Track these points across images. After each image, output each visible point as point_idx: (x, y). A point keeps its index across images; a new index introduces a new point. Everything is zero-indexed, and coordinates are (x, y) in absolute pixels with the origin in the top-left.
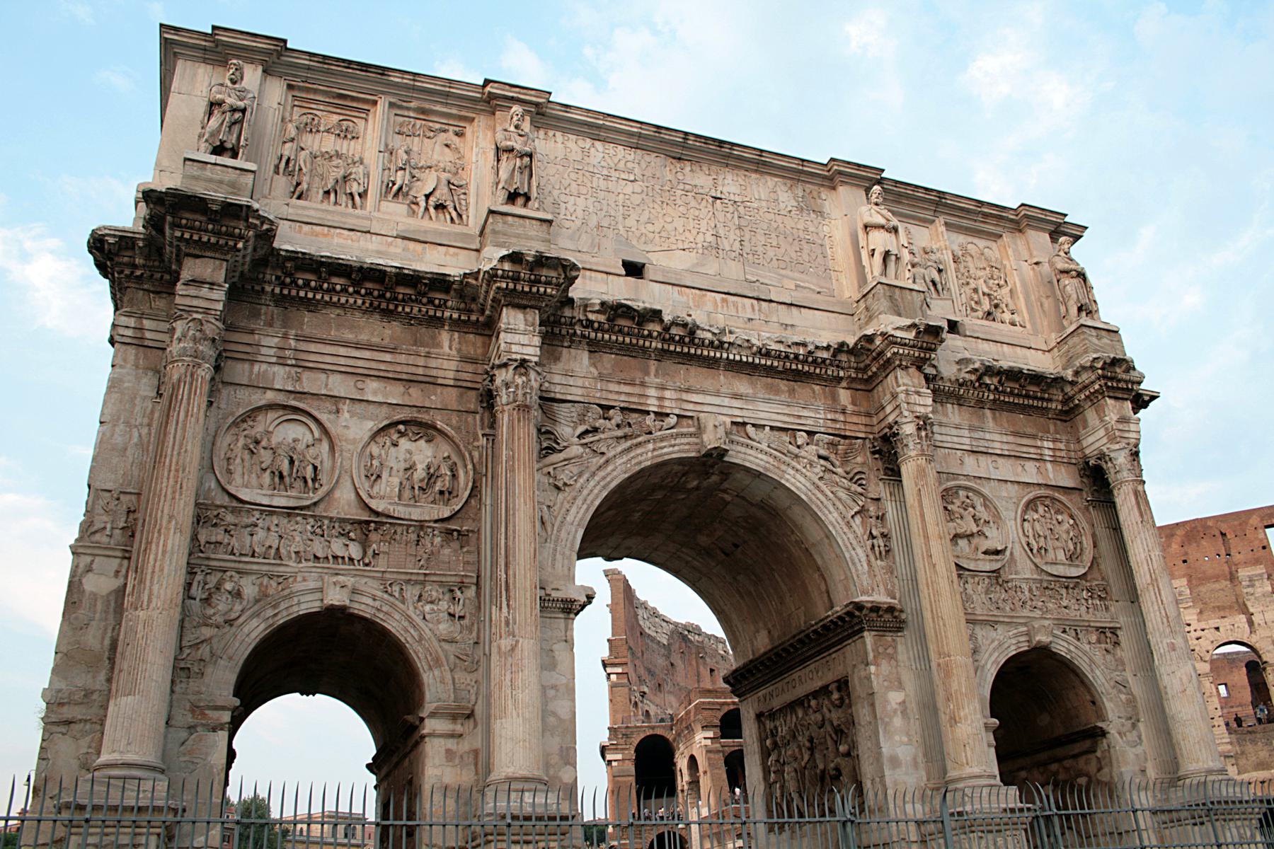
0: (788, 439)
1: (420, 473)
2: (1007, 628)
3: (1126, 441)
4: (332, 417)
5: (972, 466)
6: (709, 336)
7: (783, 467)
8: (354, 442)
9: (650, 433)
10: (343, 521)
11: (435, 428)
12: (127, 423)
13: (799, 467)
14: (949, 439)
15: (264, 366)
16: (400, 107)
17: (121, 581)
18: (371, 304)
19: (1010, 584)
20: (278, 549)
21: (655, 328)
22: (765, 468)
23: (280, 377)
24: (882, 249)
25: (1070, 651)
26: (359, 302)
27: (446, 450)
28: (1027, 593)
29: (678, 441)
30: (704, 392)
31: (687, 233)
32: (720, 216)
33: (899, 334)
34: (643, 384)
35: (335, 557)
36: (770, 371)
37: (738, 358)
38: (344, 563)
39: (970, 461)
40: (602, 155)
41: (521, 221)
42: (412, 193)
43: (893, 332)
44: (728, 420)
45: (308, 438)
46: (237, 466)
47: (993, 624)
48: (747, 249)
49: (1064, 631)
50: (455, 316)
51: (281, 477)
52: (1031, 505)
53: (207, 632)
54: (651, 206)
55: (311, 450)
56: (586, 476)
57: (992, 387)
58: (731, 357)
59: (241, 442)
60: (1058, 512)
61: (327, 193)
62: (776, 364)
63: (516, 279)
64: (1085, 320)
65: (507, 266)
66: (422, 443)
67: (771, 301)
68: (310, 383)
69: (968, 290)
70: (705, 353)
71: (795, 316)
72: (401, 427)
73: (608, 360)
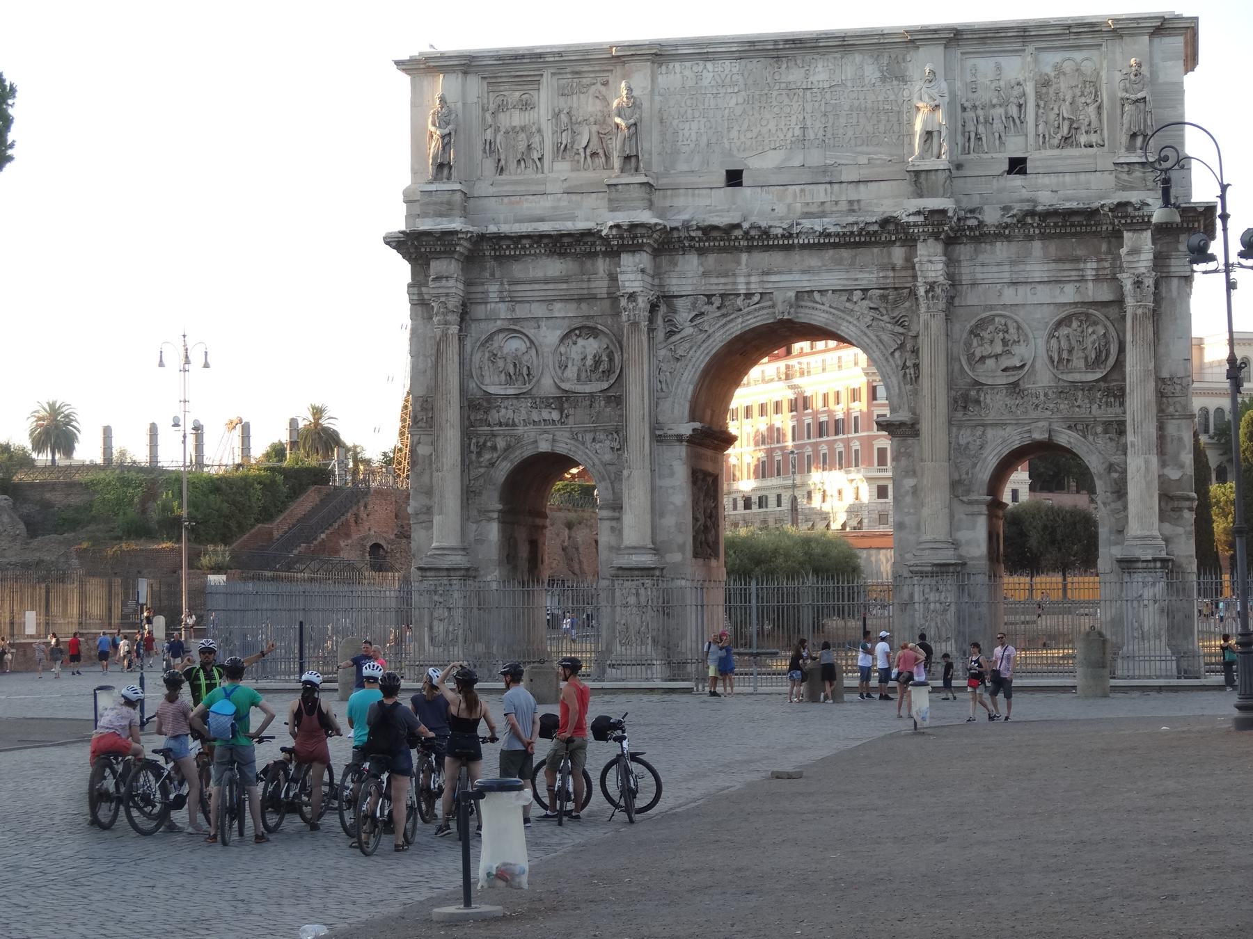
1: (589, 362)
2: (1015, 427)
3: (1133, 271)
6: (780, 231)
7: (839, 321)
9: (741, 310)
10: (547, 398)
11: (596, 328)
12: (424, 355)
13: (851, 320)
14: (990, 276)
15: (493, 305)
19: (1026, 393)
21: (738, 233)
22: (826, 324)
23: (503, 310)
25: (1070, 442)
27: (605, 342)
28: (1042, 397)
29: (761, 313)
31: (779, 132)
32: (809, 107)
33: (912, 219)
34: (734, 275)
36: (835, 246)
37: (806, 241)
40: (712, 74)
41: (627, 187)
42: (576, 147)
43: (905, 219)
44: (792, 294)
45: (524, 348)
46: (486, 373)
47: (1001, 425)
48: (829, 135)
49: (1069, 428)
50: (603, 249)
53: (482, 470)
55: (526, 358)
57: (1035, 225)
58: (801, 242)
59: (487, 355)
60: (1095, 323)
61: (519, 161)
62: (837, 240)
63: (622, 237)
65: (614, 232)
66: (591, 339)
68: (521, 311)
69: (1052, 116)
70: (781, 242)
71: (864, 193)
72: (577, 332)
73: (711, 259)
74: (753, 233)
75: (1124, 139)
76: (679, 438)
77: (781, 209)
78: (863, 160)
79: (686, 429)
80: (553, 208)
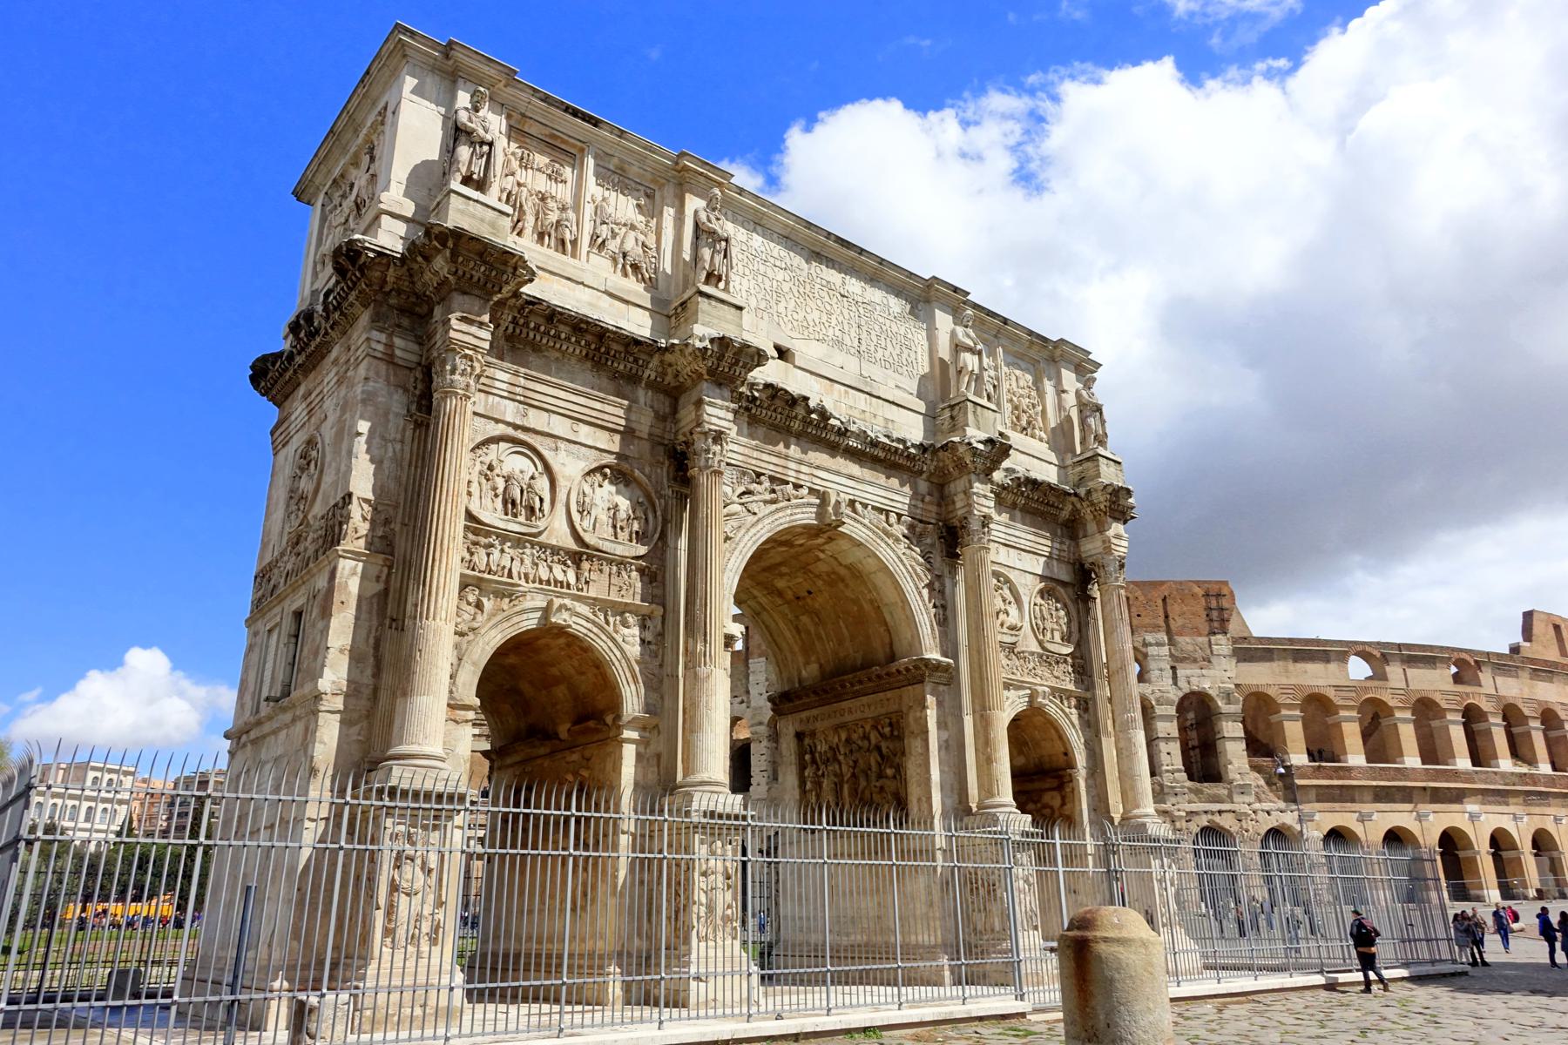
0: (883, 517)
1: (622, 515)
4: (553, 453)
6: (838, 423)
8: (569, 479)
10: (561, 549)
12: (383, 438)
15: (497, 399)
16: (601, 159)
17: (381, 586)
18: (587, 355)
20: (510, 570)
23: (510, 411)
26: (578, 352)
29: (808, 509)
30: (827, 470)
32: (846, 312)
33: (981, 447)
35: (556, 581)
38: (562, 587)
43: (975, 445)
46: (475, 488)
48: (863, 348)
50: (653, 377)
51: (514, 503)
52: (1042, 593)
54: (797, 294)
56: (743, 531)
59: (478, 467)
64: (1101, 451)
67: (879, 398)
68: (536, 419)
72: (608, 471)
74: (813, 416)
80: (590, 304)
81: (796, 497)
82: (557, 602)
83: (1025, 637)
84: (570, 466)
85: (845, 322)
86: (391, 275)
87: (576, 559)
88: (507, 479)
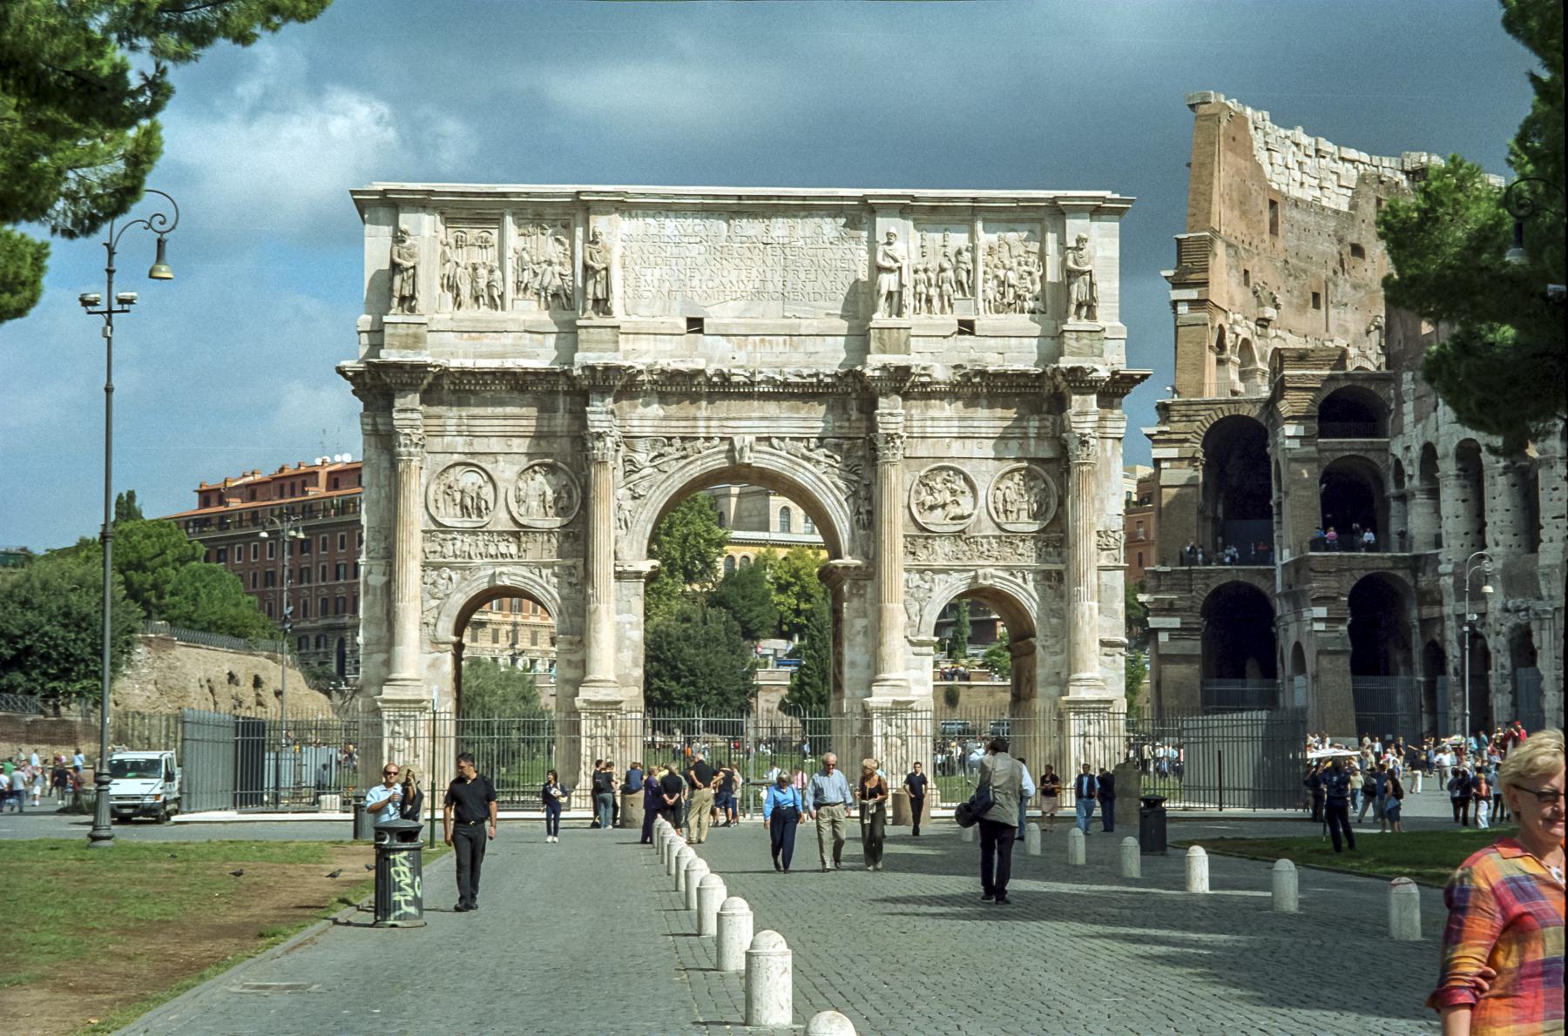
5: (957, 449)
6: (742, 379)
8: (507, 481)
12: (378, 486)
23: (460, 444)
24: (884, 291)
28: (986, 546)
30: (739, 419)
33: (877, 373)
34: (695, 419)
36: (792, 396)
39: (956, 444)
44: (753, 438)
46: (441, 504)
47: (945, 571)
49: (1012, 574)
59: (442, 488)
68: (479, 444)
72: (537, 468)
74: (715, 379)
75: (1073, 308)
76: (638, 575)
77: (742, 358)
78: (822, 313)
79: (646, 566)
80: (513, 345)
81: (708, 448)
82: (498, 570)
83: (979, 521)
84: (506, 471)
85: (767, 270)
86: (368, 380)
87: (516, 535)
88: (462, 492)
